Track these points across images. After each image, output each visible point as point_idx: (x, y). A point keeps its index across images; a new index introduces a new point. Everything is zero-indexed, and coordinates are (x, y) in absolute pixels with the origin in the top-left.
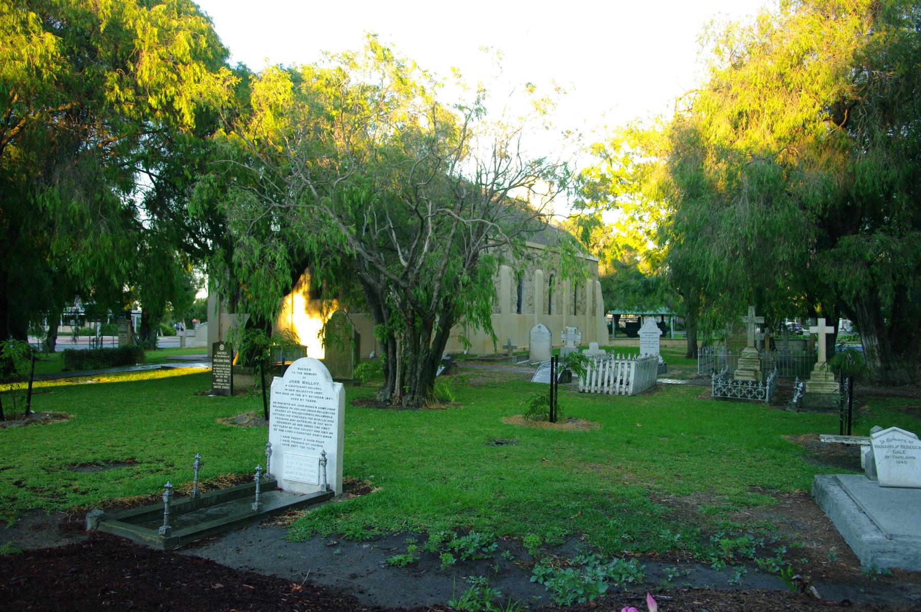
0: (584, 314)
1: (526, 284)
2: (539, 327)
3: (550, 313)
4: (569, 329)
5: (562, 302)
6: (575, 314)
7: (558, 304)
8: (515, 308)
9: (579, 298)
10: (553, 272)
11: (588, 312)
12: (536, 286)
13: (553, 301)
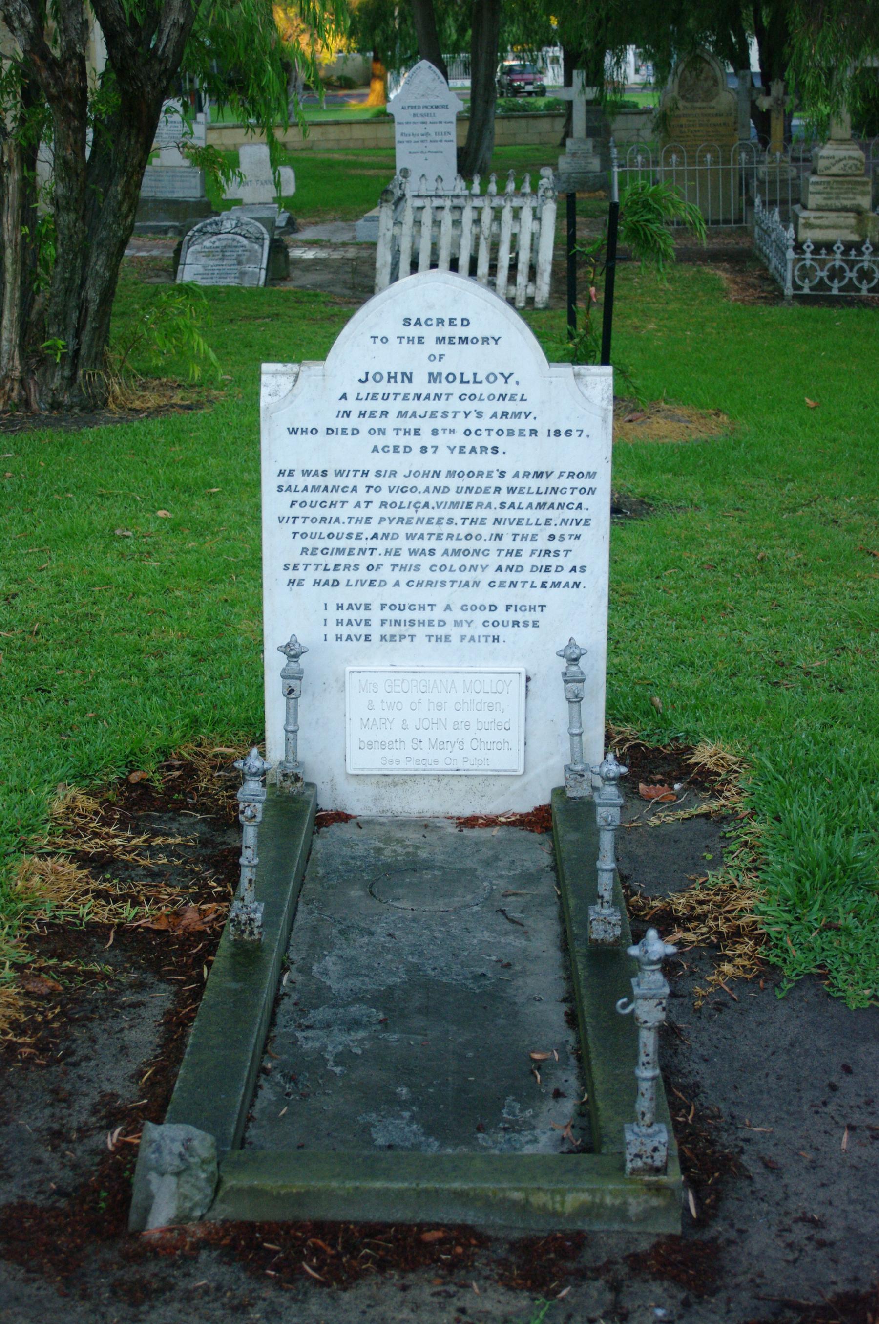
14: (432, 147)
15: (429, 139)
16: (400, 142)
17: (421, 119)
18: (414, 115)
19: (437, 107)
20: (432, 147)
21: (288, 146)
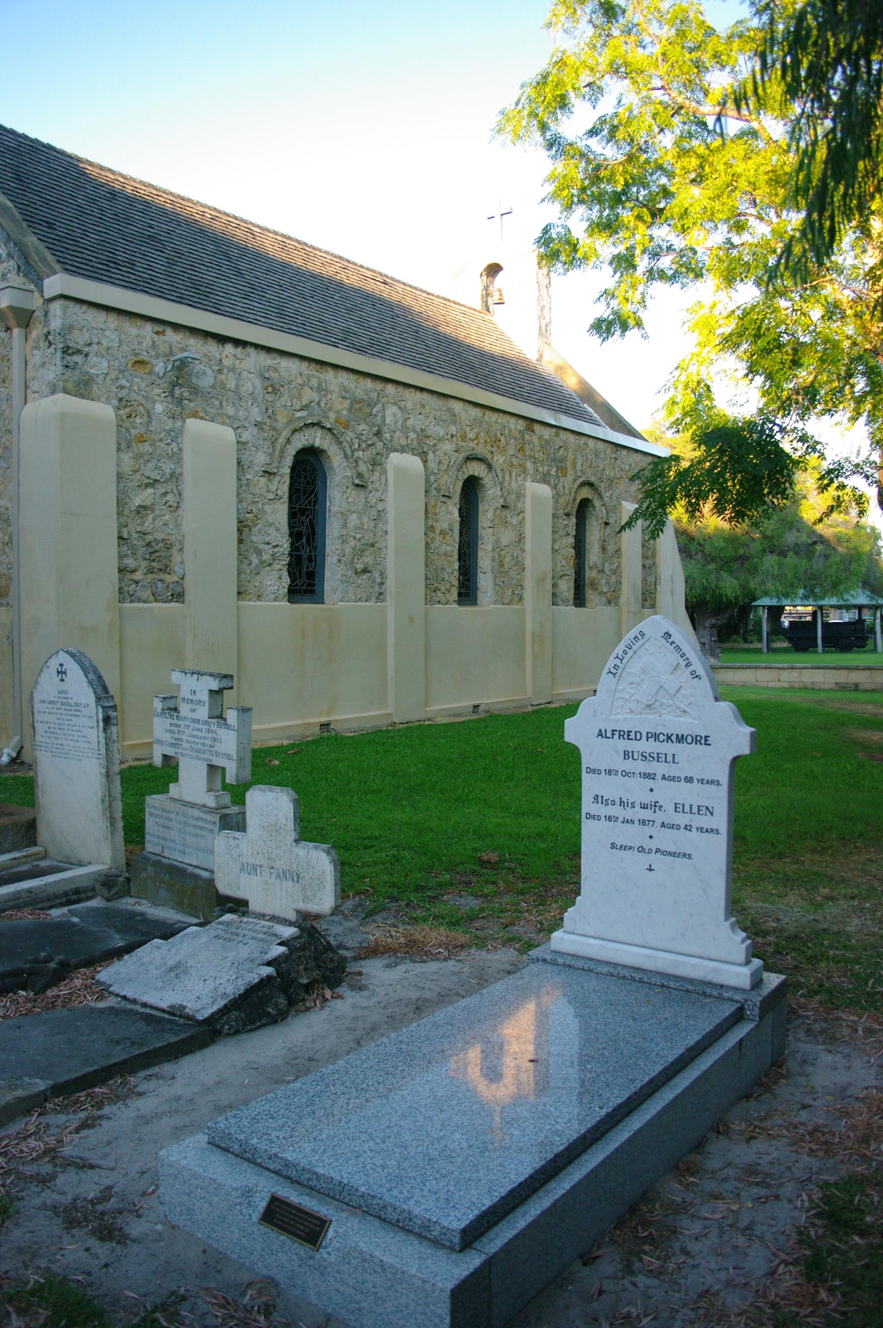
0: (612, 600)
1: (338, 497)
3: (467, 592)
6: (579, 600)
8: (277, 580)
9: (593, 555)
11: (629, 593)
13: (485, 561)
14: (666, 840)
15: (659, 817)
16: (589, 816)
17: (641, 766)
18: (627, 755)
19: (681, 739)
20: (666, 840)
21: (861, 687)
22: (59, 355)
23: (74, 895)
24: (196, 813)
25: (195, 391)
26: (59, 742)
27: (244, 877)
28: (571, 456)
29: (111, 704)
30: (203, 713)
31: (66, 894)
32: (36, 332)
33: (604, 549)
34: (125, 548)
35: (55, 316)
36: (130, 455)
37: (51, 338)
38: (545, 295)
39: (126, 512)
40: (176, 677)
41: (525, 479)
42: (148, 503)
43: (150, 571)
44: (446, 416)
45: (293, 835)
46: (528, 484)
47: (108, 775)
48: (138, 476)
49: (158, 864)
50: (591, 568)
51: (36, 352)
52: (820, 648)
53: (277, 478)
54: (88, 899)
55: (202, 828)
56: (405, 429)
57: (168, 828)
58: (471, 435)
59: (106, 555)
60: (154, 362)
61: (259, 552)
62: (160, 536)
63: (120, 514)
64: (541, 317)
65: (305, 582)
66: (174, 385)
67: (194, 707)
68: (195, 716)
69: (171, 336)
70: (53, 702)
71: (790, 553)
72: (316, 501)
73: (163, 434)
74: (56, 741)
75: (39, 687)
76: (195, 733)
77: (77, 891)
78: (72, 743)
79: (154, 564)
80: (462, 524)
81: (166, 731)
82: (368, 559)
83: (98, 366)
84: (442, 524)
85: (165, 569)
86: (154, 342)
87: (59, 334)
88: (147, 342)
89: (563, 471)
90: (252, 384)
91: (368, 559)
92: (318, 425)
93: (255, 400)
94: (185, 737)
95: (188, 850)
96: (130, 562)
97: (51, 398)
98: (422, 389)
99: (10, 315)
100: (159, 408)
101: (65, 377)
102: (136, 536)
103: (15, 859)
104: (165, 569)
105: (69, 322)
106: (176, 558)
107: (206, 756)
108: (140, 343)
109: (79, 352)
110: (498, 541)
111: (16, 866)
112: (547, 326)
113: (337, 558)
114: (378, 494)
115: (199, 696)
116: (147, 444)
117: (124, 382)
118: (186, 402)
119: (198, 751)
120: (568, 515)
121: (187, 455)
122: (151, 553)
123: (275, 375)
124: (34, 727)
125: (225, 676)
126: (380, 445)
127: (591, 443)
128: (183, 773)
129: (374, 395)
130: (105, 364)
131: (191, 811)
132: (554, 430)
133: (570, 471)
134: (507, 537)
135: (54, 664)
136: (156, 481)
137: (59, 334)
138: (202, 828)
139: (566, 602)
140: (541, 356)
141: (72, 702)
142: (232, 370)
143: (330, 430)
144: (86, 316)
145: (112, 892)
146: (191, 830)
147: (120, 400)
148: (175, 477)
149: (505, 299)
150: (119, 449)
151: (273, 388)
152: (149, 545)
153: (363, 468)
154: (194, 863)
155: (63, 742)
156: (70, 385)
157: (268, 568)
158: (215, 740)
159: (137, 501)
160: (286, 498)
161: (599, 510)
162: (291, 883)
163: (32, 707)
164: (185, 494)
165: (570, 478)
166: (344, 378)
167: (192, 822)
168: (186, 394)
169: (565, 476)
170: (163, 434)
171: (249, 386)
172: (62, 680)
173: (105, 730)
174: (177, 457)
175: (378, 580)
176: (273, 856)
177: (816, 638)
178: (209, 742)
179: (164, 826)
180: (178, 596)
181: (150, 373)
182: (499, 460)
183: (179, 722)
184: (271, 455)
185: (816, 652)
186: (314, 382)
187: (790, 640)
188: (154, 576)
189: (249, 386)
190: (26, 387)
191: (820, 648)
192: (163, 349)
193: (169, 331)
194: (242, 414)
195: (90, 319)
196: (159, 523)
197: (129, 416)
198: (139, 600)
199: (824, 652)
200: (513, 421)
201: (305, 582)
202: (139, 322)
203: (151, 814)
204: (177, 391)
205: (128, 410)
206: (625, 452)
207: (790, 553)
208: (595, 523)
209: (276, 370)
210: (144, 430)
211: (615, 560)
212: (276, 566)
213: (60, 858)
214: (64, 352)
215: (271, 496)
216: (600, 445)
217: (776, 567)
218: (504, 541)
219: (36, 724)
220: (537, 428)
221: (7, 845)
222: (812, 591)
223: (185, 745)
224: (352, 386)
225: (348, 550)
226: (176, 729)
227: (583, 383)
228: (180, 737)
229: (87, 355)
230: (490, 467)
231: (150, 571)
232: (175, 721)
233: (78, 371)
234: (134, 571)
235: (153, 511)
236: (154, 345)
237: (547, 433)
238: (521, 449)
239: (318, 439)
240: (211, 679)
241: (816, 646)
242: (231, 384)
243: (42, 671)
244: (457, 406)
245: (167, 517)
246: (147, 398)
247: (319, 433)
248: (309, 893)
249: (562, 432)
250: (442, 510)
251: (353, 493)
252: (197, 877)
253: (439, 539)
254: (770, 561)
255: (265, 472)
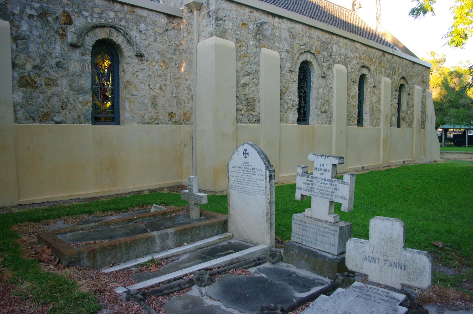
0: (410, 126)
1: (315, 81)
2: (245, 154)
3: (360, 122)
4: (318, 161)
5: (379, 110)
7: (372, 112)
8: (293, 115)
9: (404, 107)
10: (365, 71)
11: (416, 123)
12: (335, 85)
13: (366, 108)
22: (214, 20)
23: (258, 261)
24: (325, 225)
25: (264, 36)
26: (243, 186)
27: (366, 264)
28: (397, 67)
29: (272, 169)
30: (328, 175)
31: (254, 261)
32: (204, 12)
33: (408, 104)
34: (238, 101)
35: (212, 5)
36: (241, 62)
37: (210, 14)
38: (378, 4)
39: (239, 86)
40: (311, 157)
41: (381, 76)
42: (247, 82)
43: (247, 110)
44: (354, 49)
45: (402, 244)
46: (383, 78)
47: (270, 203)
48: (243, 71)
49: (300, 248)
50: (402, 112)
51: (203, 20)
52: (467, 145)
53: (294, 73)
54: (264, 263)
55: (327, 233)
56: (340, 54)
57: (306, 231)
58: (363, 57)
59: (231, 104)
60: (249, 24)
61: (287, 103)
62: (251, 96)
63: (237, 87)
64: (377, 13)
65: (303, 117)
66: (257, 34)
67: (322, 172)
68: (323, 177)
69: (256, 14)
70: (240, 167)
71: (461, 108)
72: (307, 83)
73: (253, 54)
74: (240, 185)
75: (232, 160)
76: (322, 185)
77: (259, 259)
78: (250, 187)
79: (249, 108)
80: (359, 94)
81: (304, 183)
82: (326, 107)
83: (229, 25)
84: (352, 94)
85: (253, 110)
86: (249, 16)
87: (214, 12)
88: (247, 16)
89: (394, 72)
90: (285, 34)
91: (326, 107)
92: (309, 52)
93: (286, 41)
94: (316, 187)
95: (317, 243)
96: (240, 107)
97: (211, 38)
98: (346, 38)
99: (193, 5)
100: (251, 43)
101: (216, 29)
102: (242, 96)
103: (220, 239)
104: (253, 110)
105: (218, 7)
106: (257, 105)
107: (329, 197)
108: (244, 16)
109: (221, 19)
110: (372, 100)
111: (221, 242)
112: (379, 16)
113: (315, 106)
114: (330, 81)
115: (325, 167)
116: (247, 58)
117: (238, 32)
118: (261, 41)
119: (325, 194)
120: (396, 90)
121: (262, 63)
122: (248, 103)
123: (293, 31)
124: (228, 179)
125: (341, 158)
126: (331, 60)
127: (404, 61)
128: (313, 204)
129: (329, 40)
130: (231, 25)
131: (321, 224)
132: (392, 56)
133: (397, 73)
134: (375, 99)
135: (241, 150)
136: (250, 73)
137: (214, 12)
138: (327, 233)
139: (394, 125)
140: (377, 28)
141: (252, 168)
142: (278, 28)
143: (313, 54)
144: (224, 5)
145: (275, 260)
146: (321, 233)
147: (237, 39)
148: (257, 72)
149: (361, 6)
150: (237, 60)
151: (293, 36)
152: (247, 100)
153: (325, 70)
154: (322, 249)
155: (245, 186)
156: (218, 33)
157: (290, 110)
158: (335, 189)
159: (243, 81)
160: (297, 82)
161: (407, 89)
162: (399, 270)
163: (228, 169)
164: (260, 79)
165: (397, 75)
166: (318, 33)
167: (321, 229)
168: (261, 38)
169: (395, 74)
170: (253, 54)
171: (284, 35)
172: (246, 157)
173: (270, 182)
174: (257, 64)
175: (330, 116)
176: (388, 254)
177: (465, 141)
178: (331, 190)
179: (303, 230)
180: (258, 121)
181: (248, 29)
182: (372, 68)
183: (312, 180)
184: (292, 64)
185: (465, 147)
186: (308, 34)
187: (454, 142)
188: (249, 112)
189: (284, 35)
190: (199, 35)
191: (467, 145)
192: (253, 19)
193: (255, 12)
194: (281, 46)
195: (226, 6)
196: (251, 91)
197: (240, 46)
198: (243, 122)
199: (468, 146)
200: (377, 51)
201: (303, 117)
202: (244, 8)
203: (296, 223)
204: (258, 36)
205: (239, 44)
206: (416, 65)
207: (461, 108)
208: (405, 94)
209: (294, 29)
210: (245, 52)
211: (412, 109)
212: (293, 109)
213: (240, 239)
214: (216, 19)
215: (292, 80)
216: (408, 62)
217: (455, 113)
218: (374, 101)
219: (230, 177)
220: (386, 55)
221: (215, 232)
222: (470, 123)
223: (315, 191)
224: (321, 36)
225: (319, 104)
226: (310, 183)
227: (394, 39)
228: (313, 187)
229: (224, 21)
230: (369, 70)
231: (247, 110)
232: (310, 179)
233: (221, 27)
234: (241, 110)
235: (249, 85)
236: (249, 17)
237: (389, 57)
238: (380, 64)
239: (309, 57)
240: (334, 159)
241: (465, 144)
242: (278, 34)
243: (234, 152)
244: (358, 45)
245: (254, 88)
246: (246, 39)
247: (309, 55)
248: (412, 277)
249: (395, 57)
250: (352, 87)
251: (321, 79)
252: (325, 257)
253: (351, 99)
254: (453, 111)
255: (290, 70)
